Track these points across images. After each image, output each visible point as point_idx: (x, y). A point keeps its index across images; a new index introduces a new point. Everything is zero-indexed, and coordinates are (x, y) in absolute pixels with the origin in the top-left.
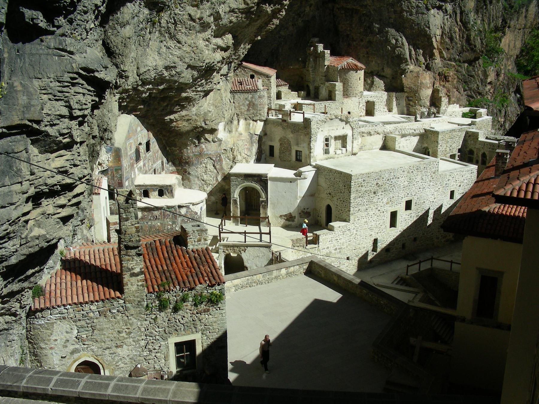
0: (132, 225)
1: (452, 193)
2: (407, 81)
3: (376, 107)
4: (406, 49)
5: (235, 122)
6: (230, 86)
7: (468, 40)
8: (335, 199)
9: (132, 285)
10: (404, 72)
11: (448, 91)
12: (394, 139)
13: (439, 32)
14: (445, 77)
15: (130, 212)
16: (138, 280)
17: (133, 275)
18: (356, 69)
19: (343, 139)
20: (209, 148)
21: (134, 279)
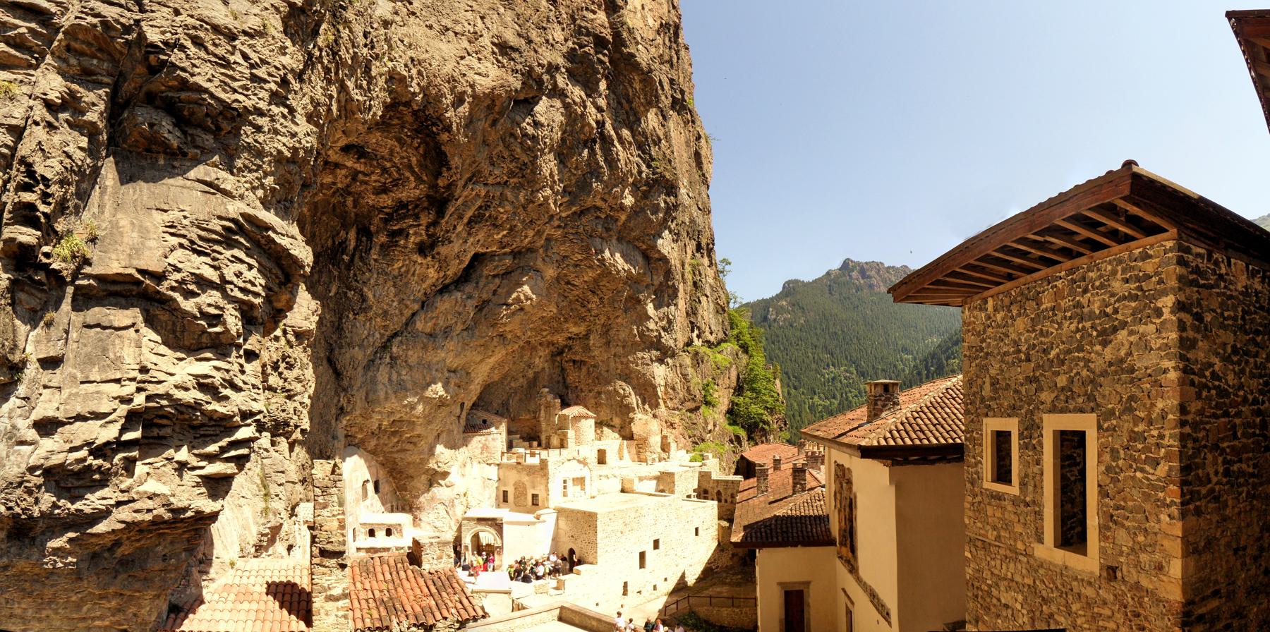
0: (334, 516)
1: (697, 529)
2: (636, 429)
3: (607, 455)
4: (633, 400)
5: (469, 465)
6: (462, 429)
7: (688, 390)
8: (579, 541)
9: (327, 614)
10: (632, 420)
11: (676, 437)
12: (631, 481)
13: (663, 383)
14: (672, 424)
15: (331, 494)
16: (338, 609)
17: (331, 598)
18: (587, 417)
19: (580, 481)
20: (439, 492)
21: (331, 605)
